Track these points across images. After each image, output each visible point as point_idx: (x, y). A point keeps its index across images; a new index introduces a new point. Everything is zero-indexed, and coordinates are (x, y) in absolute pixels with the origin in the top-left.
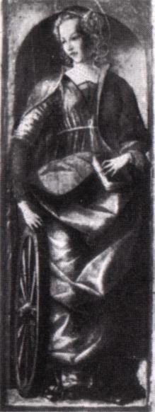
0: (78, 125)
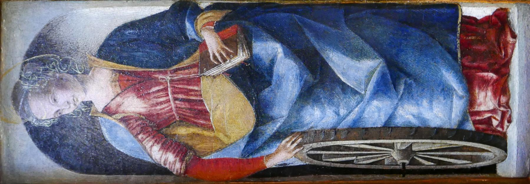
0: (168, 95)
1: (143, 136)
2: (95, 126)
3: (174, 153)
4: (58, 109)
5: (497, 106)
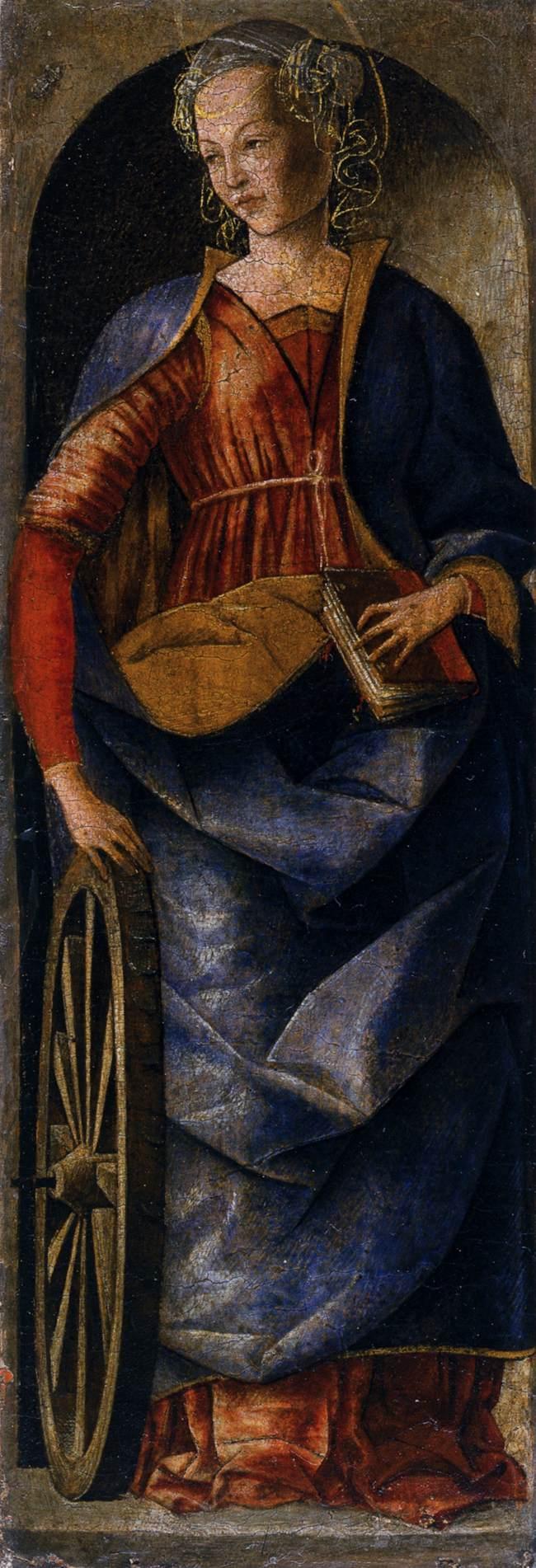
1: (144, 402)
3: (91, 493)
5: (226, 1468)
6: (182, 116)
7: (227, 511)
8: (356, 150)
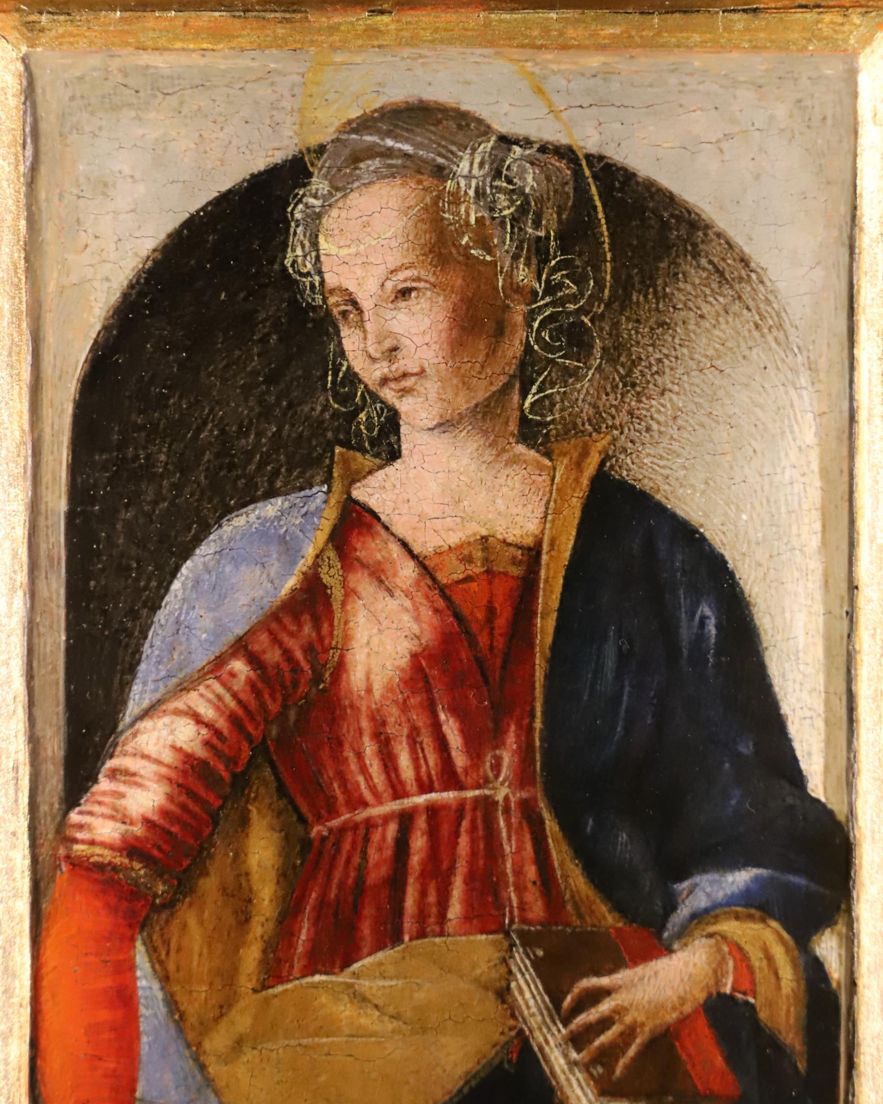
0: (425, 787)
1: (242, 678)
2: (289, 471)
3: (164, 813)
4: (366, 304)
6: (299, 252)
7: (367, 839)
8: (562, 302)
